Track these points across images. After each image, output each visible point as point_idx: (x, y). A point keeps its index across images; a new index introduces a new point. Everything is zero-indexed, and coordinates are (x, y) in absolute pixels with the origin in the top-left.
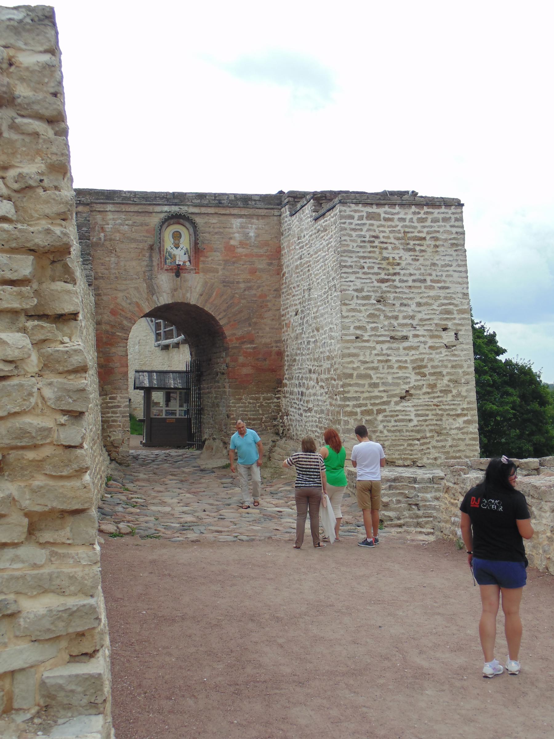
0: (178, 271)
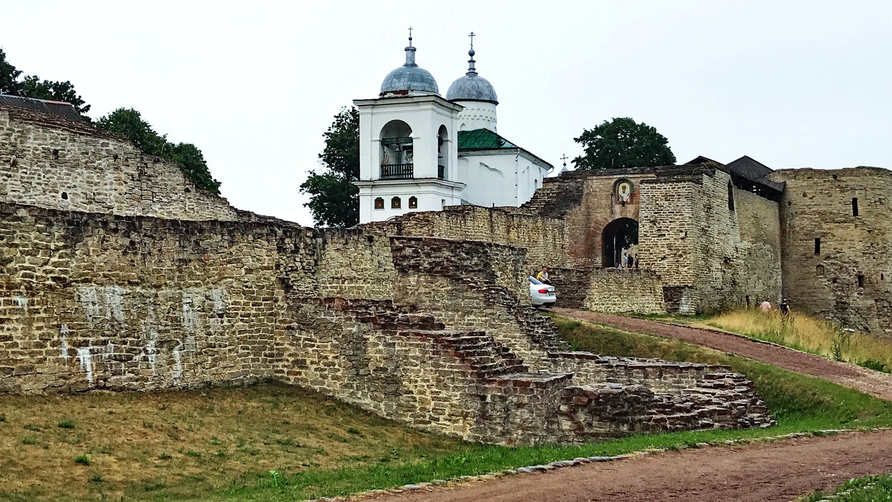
0: (623, 204)
